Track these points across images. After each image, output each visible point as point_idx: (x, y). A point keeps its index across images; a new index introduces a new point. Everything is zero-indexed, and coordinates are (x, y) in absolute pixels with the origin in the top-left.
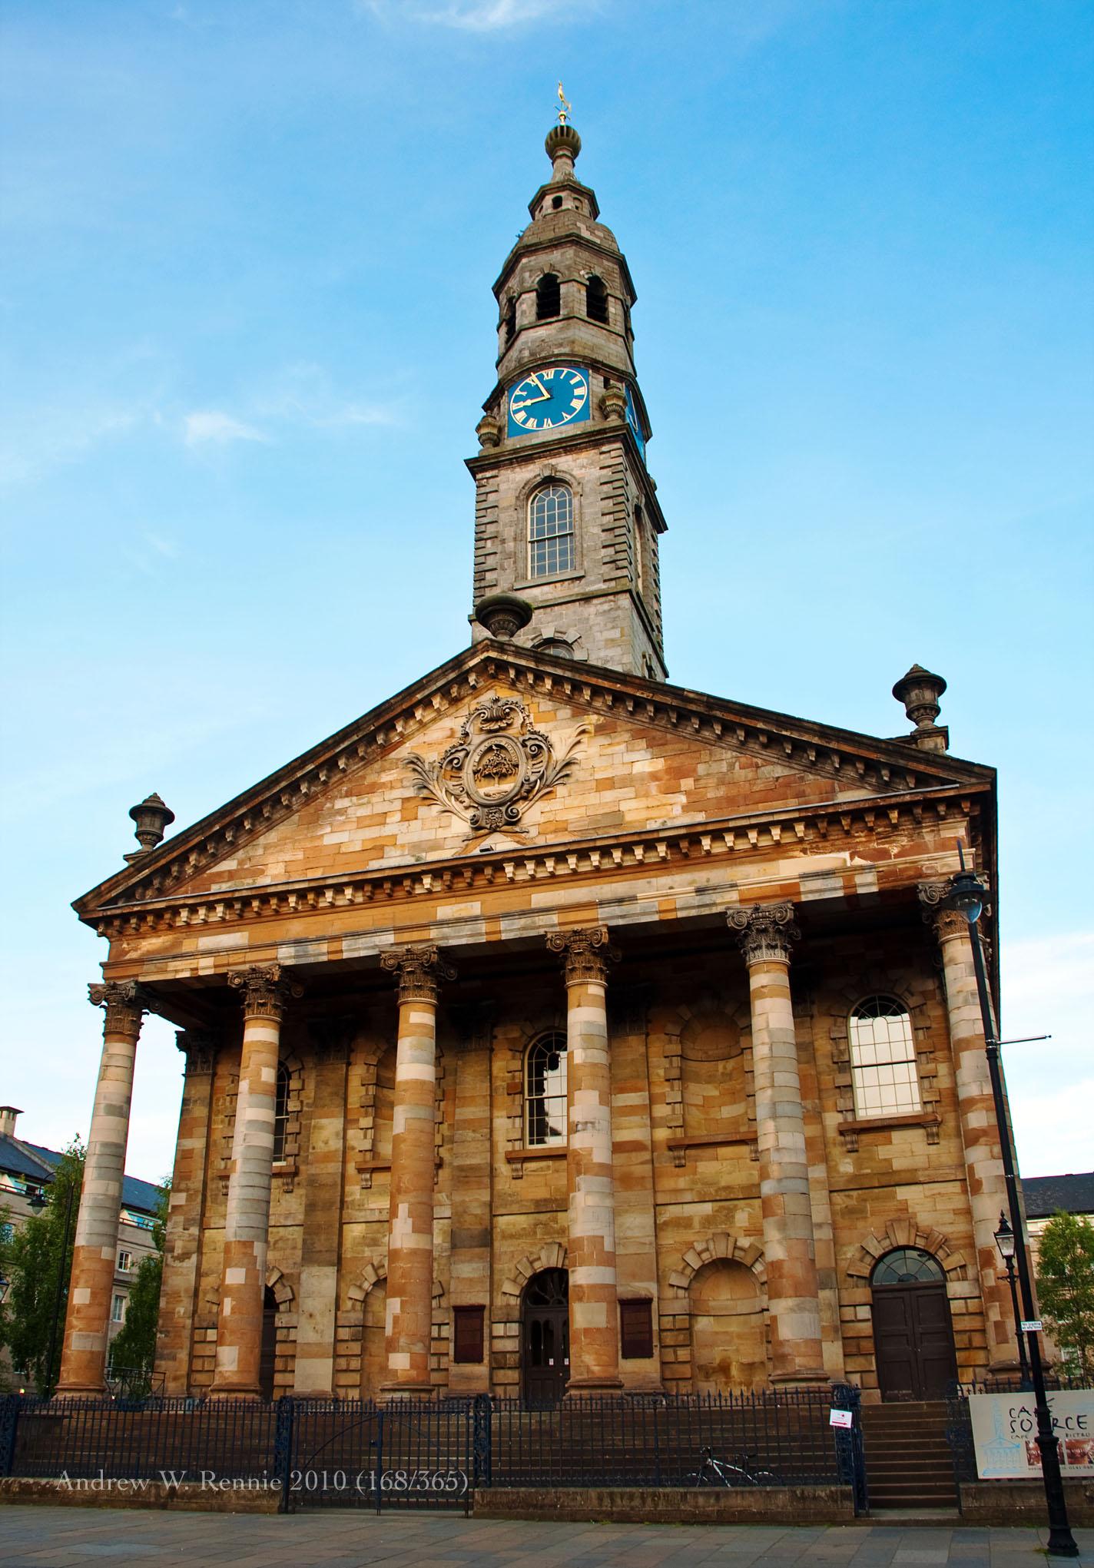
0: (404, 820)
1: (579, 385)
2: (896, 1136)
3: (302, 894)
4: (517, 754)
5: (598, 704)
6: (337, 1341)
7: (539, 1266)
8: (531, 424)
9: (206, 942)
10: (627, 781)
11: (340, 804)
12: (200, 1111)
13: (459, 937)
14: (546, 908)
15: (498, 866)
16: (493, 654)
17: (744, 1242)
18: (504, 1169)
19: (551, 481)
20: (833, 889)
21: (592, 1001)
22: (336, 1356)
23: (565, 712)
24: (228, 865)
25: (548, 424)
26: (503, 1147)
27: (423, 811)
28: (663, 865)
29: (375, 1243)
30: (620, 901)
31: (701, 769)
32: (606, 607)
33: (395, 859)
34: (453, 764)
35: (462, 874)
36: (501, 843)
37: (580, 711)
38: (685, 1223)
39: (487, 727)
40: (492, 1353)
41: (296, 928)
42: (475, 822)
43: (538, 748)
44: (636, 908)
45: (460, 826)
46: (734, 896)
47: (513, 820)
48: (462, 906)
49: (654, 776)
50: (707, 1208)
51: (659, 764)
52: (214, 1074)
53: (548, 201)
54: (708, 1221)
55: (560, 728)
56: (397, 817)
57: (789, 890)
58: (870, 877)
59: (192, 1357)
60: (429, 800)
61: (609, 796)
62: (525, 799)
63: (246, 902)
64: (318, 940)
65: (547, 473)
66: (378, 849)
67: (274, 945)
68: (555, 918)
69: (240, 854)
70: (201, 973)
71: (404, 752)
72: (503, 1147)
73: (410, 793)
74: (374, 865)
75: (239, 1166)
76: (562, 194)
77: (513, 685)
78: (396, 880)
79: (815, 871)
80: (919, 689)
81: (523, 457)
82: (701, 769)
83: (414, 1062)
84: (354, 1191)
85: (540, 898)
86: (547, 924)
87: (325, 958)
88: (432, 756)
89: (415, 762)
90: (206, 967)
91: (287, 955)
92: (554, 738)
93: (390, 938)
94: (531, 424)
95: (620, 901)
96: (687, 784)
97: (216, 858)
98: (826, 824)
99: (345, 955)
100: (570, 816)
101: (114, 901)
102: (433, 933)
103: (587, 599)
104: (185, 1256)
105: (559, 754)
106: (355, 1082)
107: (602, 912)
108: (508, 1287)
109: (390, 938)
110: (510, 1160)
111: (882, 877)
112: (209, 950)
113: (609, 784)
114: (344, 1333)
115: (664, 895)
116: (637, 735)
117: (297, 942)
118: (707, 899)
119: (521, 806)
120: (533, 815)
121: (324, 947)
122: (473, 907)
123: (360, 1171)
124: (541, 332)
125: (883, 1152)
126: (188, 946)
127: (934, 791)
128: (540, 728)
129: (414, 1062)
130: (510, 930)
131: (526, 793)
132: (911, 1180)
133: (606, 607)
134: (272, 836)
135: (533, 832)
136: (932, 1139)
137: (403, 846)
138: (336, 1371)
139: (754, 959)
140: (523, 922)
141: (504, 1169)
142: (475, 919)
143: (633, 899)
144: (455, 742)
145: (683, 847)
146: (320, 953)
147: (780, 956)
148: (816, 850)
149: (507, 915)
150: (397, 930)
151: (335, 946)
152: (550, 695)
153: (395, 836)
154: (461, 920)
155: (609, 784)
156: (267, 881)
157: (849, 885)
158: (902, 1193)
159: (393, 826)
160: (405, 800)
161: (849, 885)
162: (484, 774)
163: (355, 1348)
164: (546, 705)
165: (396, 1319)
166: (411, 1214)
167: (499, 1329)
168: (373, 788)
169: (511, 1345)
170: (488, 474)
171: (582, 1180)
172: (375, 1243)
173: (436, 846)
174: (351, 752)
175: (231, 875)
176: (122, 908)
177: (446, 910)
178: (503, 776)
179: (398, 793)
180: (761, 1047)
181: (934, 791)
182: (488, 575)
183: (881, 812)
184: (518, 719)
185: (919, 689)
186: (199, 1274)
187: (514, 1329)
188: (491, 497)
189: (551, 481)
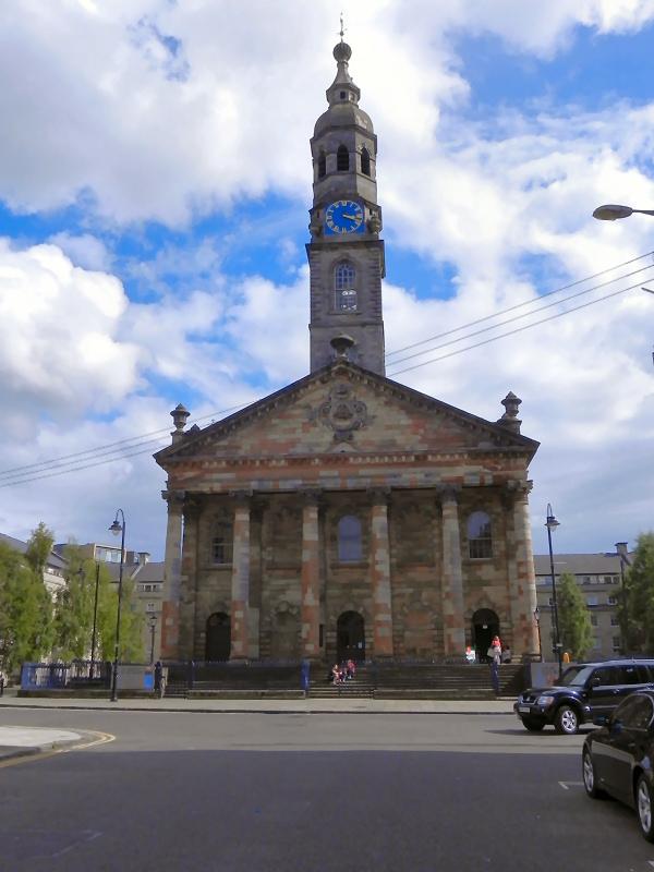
0: (304, 432)
1: (359, 212)
2: (485, 567)
4: (351, 409)
5: (387, 393)
6: (261, 638)
7: (344, 610)
8: (336, 229)
9: (216, 476)
10: (398, 427)
11: (274, 421)
12: (192, 541)
13: (329, 485)
14: (365, 476)
15: (346, 459)
16: (342, 366)
17: (426, 604)
18: (329, 570)
19: (345, 261)
20: (476, 481)
22: (260, 644)
23: (372, 394)
25: (344, 230)
26: (329, 562)
27: (312, 429)
28: (413, 465)
29: (274, 598)
30: (395, 476)
31: (427, 426)
32: (372, 330)
33: (300, 450)
34: (324, 411)
35: (330, 460)
36: (346, 447)
37: (378, 395)
38: (401, 596)
39: (340, 396)
40: (327, 644)
41: (258, 474)
42: (335, 437)
43: (361, 408)
45: (328, 437)
46: (439, 479)
47: (351, 437)
49: (408, 426)
50: (411, 590)
51: (410, 422)
52: (198, 526)
53: (338, 93)
54: (412, 595)
55: (374, 405)
56: (300, 430)
57: (460, 479)
58: (490, 477)
59: (195, 644)
60: (315, 425)
61: (390, 432)
62: (356, 429)
63: (236, 462)
64: (269, 480)
65: (345, 257)
66: (293, 444)
68: (369, 480)
69: (229, 438)
71: (301, 402)
72: (329, 562)
73: (306, 420)
74: (291, 450)
75: (239, 571)
76: (346, 91)
77: (349, 379)
78: (304, 460)
79: (468, 472)
80: (511, 402)
81: (333, 247)
82: (427, 426)
83: (310, 532)
84: (266, 577)
85: (362, 472)
86: (365, 483)
88: (315, 406)
89: (308, 407)
90: (217, 487)
91: (254, 485)
92: (368, 405)
94: (336, 229)
95: (395, 476)
96: (422, 431)
97: (218, 440)
98: (476, 456)
101: (171, 456)
102: (318, 482)
103: (364, 325)
104: (189, 602)
105: (370, 412)
106: (264, 532)
107: (388, 480)
108: (332, 618)
109: (300, 482)
110: (333, 567)
111: (494, 477)
112: (217, 480)
113: (389, 427)
114: (263, 635)
115: (413, 476)
116: (402, 408)
117: (261, 480)
118: (429, 478)
119: (355, 433)
120: (359, 436)
121: (271, 483)
122: (335, 473)
123: (268, 569)
124: (340, 178)
125: (479, 573)
126: (207, 476)
127: (515, 448)
128: (362, 399)
129: (310, 532)
130: (351, 484)
131: (356, 427)
132: (488, 583)
133: (372, 330)
134: (244, 432)
135: (359, 444)
136: (497, 569)
138: (261, 650)
139: (444, 506)
140: (355, 481)
141: (329, 570)
142: (335, 477)
143: (400, 475)
144: (324, 401)
145: (421, 460)
146: (269, 486)
147: (455, 504)
148: (471, 464)
149: (350, 477)
150: (303, 479)
152: (365, 386)
153: (299, 439)
154: (330, 478)
155: (389, 427)
156: (242, 453)
157: (482, 479)
158: (485, 589)
159: (299, 434)
160: (304, 424)
161: (482, 479)
162: (336, 416)
163: (267, 641)
164: (363, 390)
165: (308, 633)
166: (313, 591)
167: (329, 634)
168: (290, 417)
169: (334, 640)
170: (316, 252)
171: (380, 582)
172: (274, 598)
173: (318, 445)
174: (281, 401)
175: (225, 448)
176: (175, 459)
177: (323, 473)
178: (345, 418)
179: (300, 420)
180: (446, 538)
181: (515, 448)
182: (318, 305)
183: (496, 453)
184: (352, 396)
185: (511, 402)
186: (196, 610)
187: (335, 634)
188: (318, 265)
189: (345, 261)
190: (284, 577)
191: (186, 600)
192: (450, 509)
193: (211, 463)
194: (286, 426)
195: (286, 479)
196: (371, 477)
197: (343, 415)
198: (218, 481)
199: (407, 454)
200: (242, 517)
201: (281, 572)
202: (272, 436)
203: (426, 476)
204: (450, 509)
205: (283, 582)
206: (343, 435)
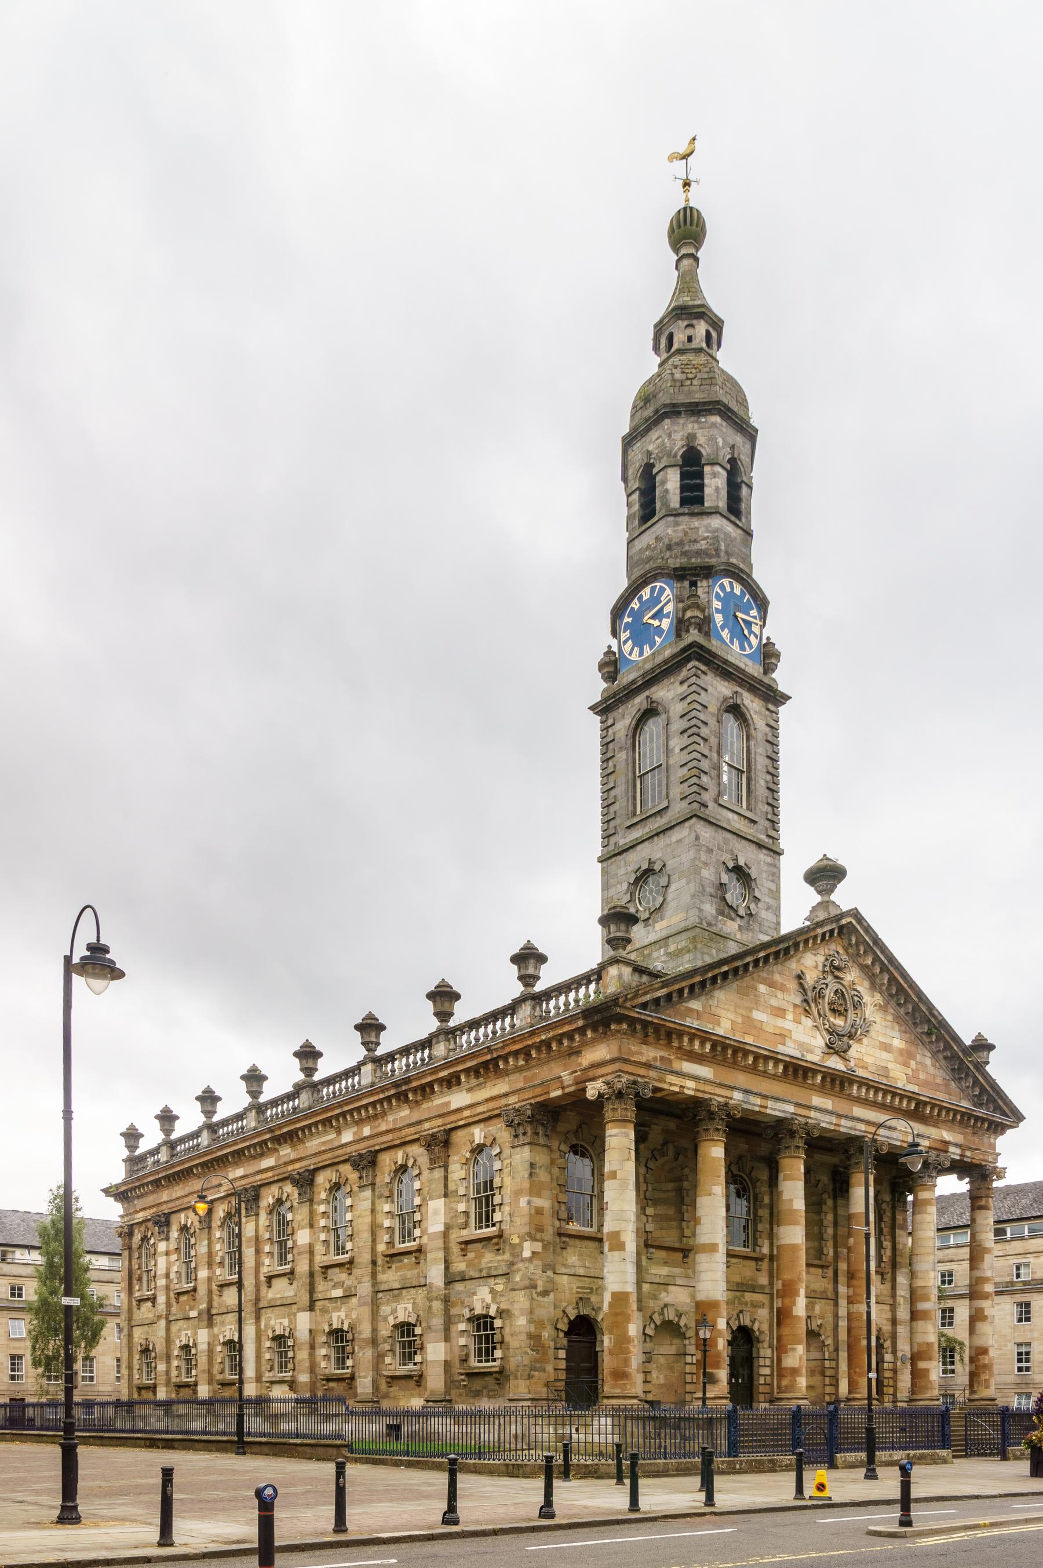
3: (757, 1057)
13: (826, 1122)
29: (655, 1297)
44: (894, 1135)
48: (823, 1100)
49: (901, 1051)
56: (790, 1016)
67: (732, 1088)
70: (686, 1091)
85: (858, 1111)
87: (757, 1109)
90: (690, 1088)
93: (791, 1108)
96: (913, 1063)
99: (768, 1111)
100: (869, 1060)
109: (791, 1108)
121: (758, 1101)
137: (795, 1041)
150: (797, 1105)
151: (764, 1102)
177: (817, 1100)
190: (666, 1263)
191: (540, 1289)
193: (692, 1038)
194: (774, 1002)
195: (777, 1099)
196: (868, 1123)
198: (695, 1078)
199: (910, 1097)
200: (715, 1153)
201: (662, 1254)
205: (664, 1271)
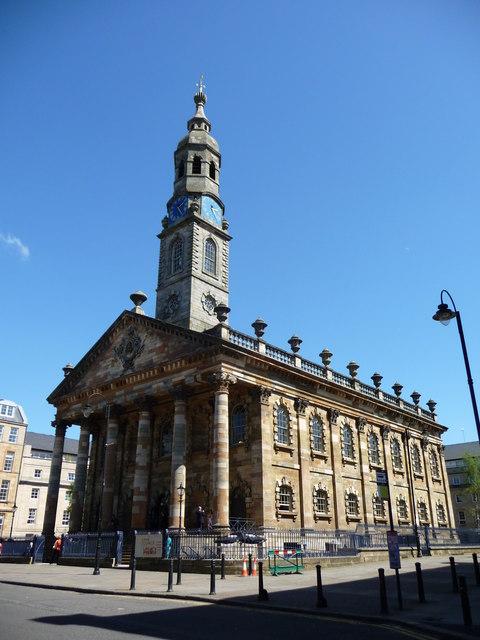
21: (145, 418)
24: (79, 384)
31: (170, 344)
35: (120, 383)
82: (170, 344)
103: (182, 279)
115: (157, 386)
116: (158, 334)
120: (137, 362)
131: (134, 357)
143: (150, 387)
189: (178, 239)
192: (178, 405)
197: (129, 350)
202: (99, 374)
203: (165, 383)
204: (178, 405)
206: (129, 364)
